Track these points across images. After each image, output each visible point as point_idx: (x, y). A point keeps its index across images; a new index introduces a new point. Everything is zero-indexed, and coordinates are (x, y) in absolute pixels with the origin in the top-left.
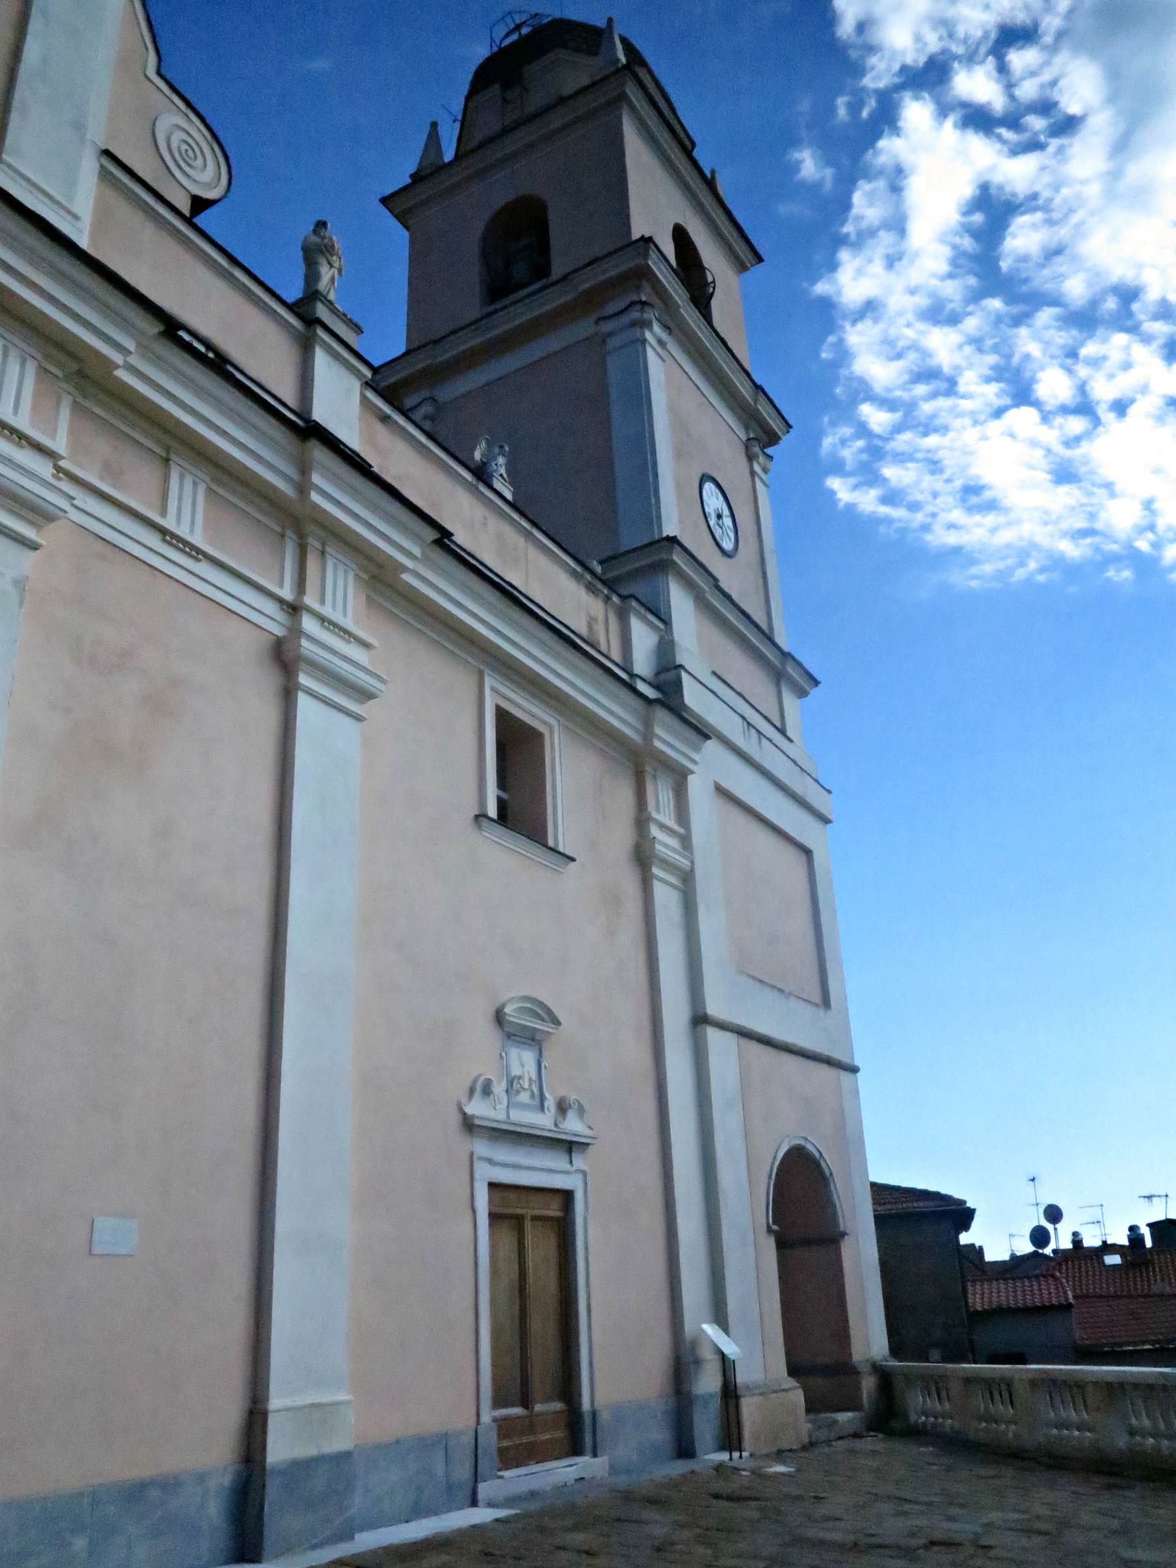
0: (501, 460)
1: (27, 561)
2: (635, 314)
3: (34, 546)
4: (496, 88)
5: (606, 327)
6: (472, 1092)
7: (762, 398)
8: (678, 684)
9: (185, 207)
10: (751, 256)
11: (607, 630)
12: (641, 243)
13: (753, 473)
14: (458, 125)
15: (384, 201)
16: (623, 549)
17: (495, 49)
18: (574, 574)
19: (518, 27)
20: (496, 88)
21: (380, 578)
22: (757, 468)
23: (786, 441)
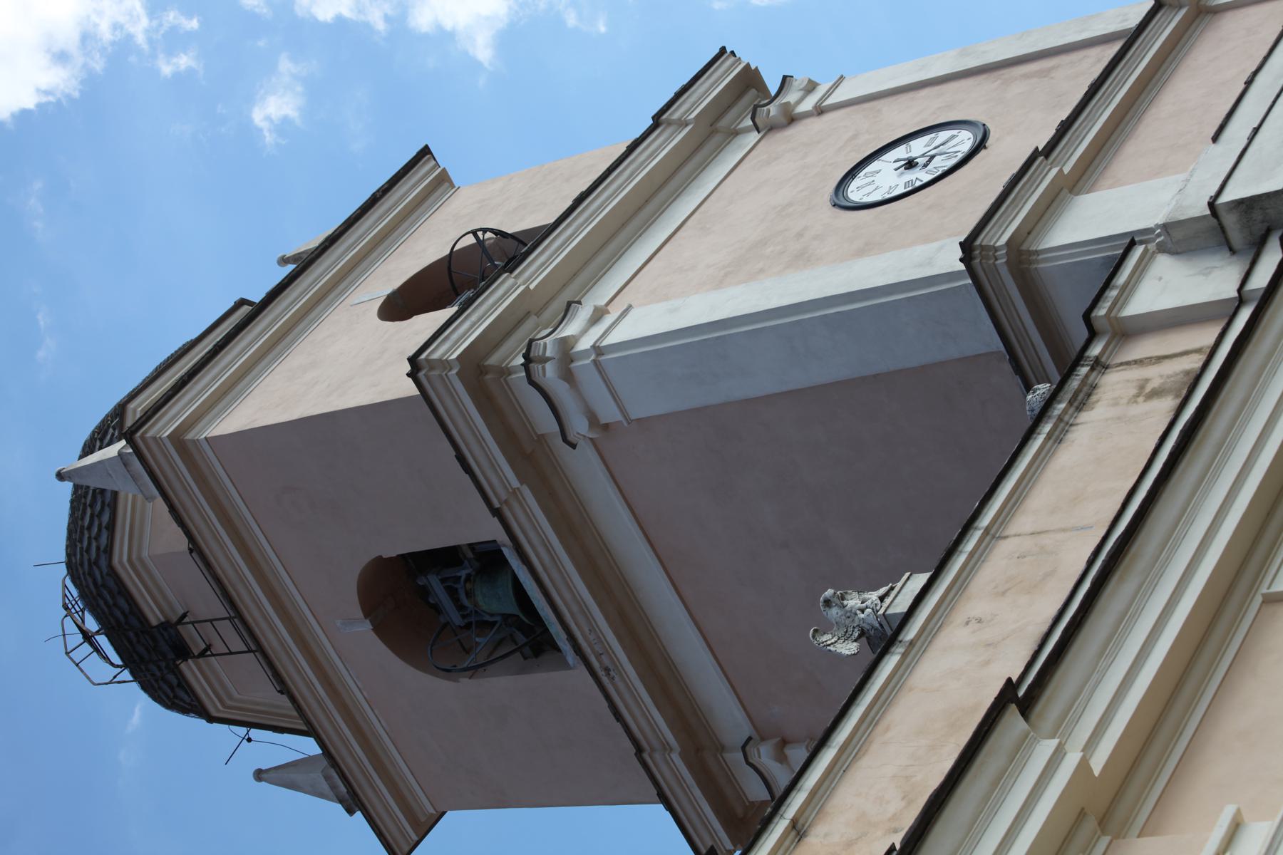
0: (853, 602)
2: (549, 374)
4: (189, 669)
5: (579, 426)
7: (675, 114)
8: (1247, 205)
10: (424, 168)
11: (1160, 359)
12: (421, 375)
13: (820, 111)
14: (254, 733)
16: (998, 344)
17: (126, 675)
18: (1057, 438)
19: (88, 637)
20: (189, 669)
22: (808, 105)
23: (749, 56)
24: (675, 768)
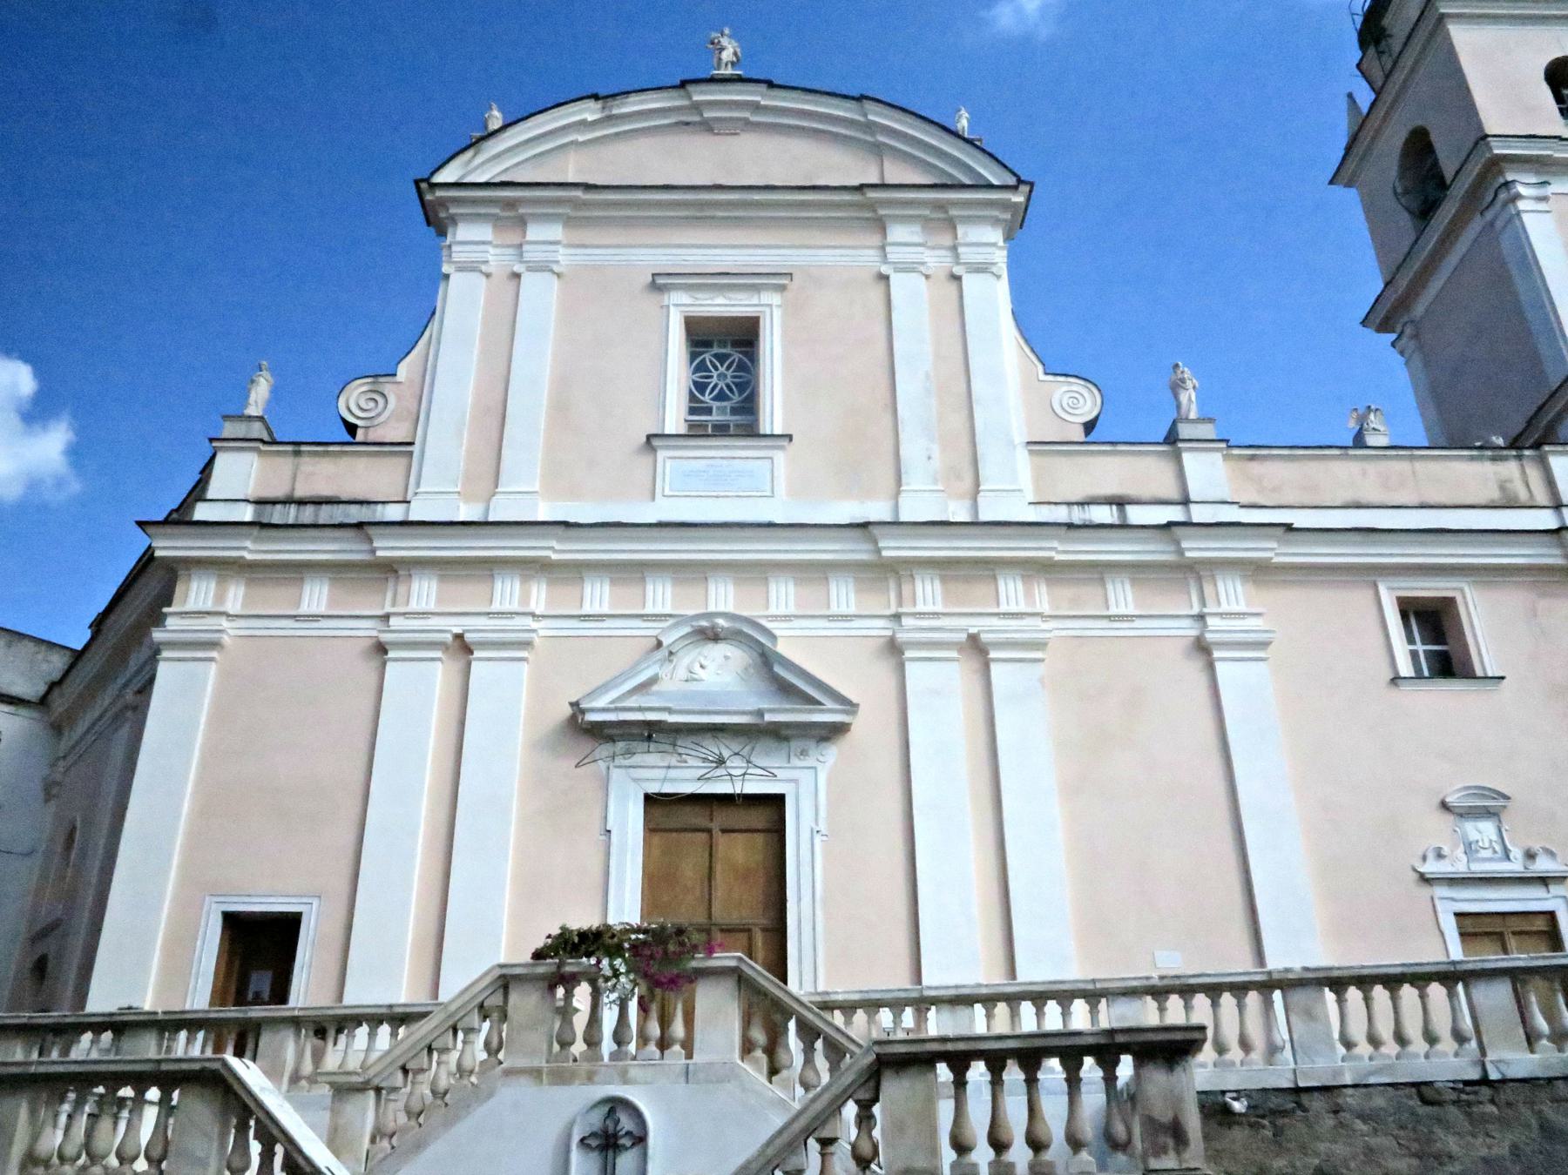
1: (1040, 669)
2: (1503, 196)
3: (1042, 660)
4: (1371, 51)
5: (1489, 215)
6: (1424, 858)
9: (1079, 435)
15: (1331, 182)
17: (1359, 20)
18: (1472, 458)
21: (1258, 572)
24: (1393, 297)
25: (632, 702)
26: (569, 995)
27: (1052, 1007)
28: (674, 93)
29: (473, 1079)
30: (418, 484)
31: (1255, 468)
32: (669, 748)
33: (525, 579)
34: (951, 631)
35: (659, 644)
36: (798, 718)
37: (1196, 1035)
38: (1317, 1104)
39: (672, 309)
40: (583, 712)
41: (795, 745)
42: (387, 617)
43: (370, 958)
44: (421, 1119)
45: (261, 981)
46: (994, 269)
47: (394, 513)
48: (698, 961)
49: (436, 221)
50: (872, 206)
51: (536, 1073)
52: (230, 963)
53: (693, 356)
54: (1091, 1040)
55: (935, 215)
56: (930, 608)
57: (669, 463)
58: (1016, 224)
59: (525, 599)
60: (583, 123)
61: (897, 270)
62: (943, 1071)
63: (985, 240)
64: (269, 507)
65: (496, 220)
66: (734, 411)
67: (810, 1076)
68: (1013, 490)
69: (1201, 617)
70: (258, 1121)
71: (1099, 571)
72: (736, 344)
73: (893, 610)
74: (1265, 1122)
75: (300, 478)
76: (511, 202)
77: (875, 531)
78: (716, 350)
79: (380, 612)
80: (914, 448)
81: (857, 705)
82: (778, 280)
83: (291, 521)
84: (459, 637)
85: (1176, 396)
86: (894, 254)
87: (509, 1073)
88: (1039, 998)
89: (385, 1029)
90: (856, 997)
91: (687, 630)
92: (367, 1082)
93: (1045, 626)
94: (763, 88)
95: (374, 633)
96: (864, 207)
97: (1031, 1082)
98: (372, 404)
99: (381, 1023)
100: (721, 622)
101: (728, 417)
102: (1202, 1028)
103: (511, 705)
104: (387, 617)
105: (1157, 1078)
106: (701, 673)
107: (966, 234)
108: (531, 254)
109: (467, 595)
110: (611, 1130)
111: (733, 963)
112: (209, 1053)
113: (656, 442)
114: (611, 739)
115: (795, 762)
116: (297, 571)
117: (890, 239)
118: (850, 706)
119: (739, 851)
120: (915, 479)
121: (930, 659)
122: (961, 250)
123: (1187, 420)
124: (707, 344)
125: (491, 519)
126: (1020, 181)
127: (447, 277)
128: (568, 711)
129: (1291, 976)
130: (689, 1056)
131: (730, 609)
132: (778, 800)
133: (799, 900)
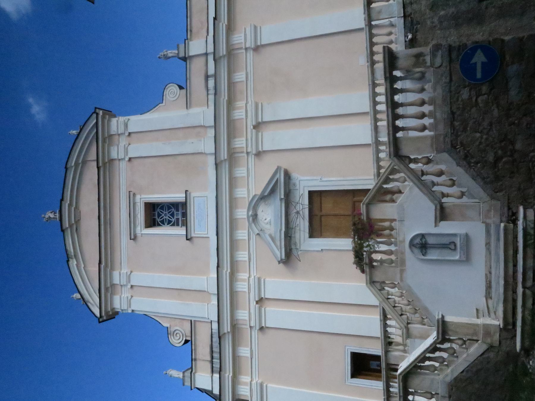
9: (184, 91)
21: (230, 29)
25: (278, 243)
26: (376, 261)
27: (378, 99)
28: (66, 233)
29: (404, 292)
30: (205, 318)
31: (194, 30)
32: (293, 230)
33: (237, 280)
34: (252, 134)
35: (258, 234)
36: (282, 187)
37: (386, 49)
38: (409, 10)
39: (143, 232)
40: (282, 259)
41: (292, 188)
42: (251, 327)
43: (365, 329)
44: (417, 309)
45: (373, 365)
46: (126, 121)
47: (215, 326)
48: (364, 217)
49: (113, 315)
50: (104, 164)
51: (402, 271)
52: (366, 375)
53: (159, 225)
54: (388, 84)
55: (107, 141)
56: (244, 142)
57: (196, 233)
58: (110, 114)
59: (244, 280)
60: (77, 265)
61: (127, 154)
62: (400, 134)
63: (116, 124)
64: (214, 369)
65: (112, 294)
66: (178, 210)
67: (402, 179)
68: (202, 114)
69: (246, 49)
70: (419, 362)
71: (231, 85)
72: (154, 210)
73: (246, 155)
74: (415, 27)
75: (204, 358)
76: (106, 289)
77: (218, 161)
78: (156, 217)
79: (249, 329)
80: (188, 148)
81: (278, 167)
82: (132, 196)
83: (219, 361)
84: (257, 302)
85: (169, 58)
86: (121, 156)
87: (402, 280)
88: (375, 103)
89: (388, 322)
90: (375, 165)
91: (253, 225)
92: (406, 327)
93: (250, 103)
94: (63, 202)
95: (256, 331)
96: (105, 166)
97: (402, 105)
98: (178, 335)
99: (386, 324)
100: (250, 213)
101: (180, 212)
102: (384, 47)
103: (280, 284)
104: (251, 327)
105: (401, 63)
106: (268, 219)
107: (114, 131)
108: (123, 282)
109: (242, 300)
110: (420, 246)
111: (365, 206)
112: (397, 380)
113: (189, 237)
114: (291, 250)
115: (298, 187)
116: (236, 358)
117: (116, 157)
118: (278, 169)
119: (328, 206)
120: (201, 149)
121: (262, 142)
122: (119, 133)
123: (178, 54)
124: (154, 219)
125: (216, 293)
126: (95, 112)
127: (133, 311)
128: (281, 264)
129: (367, 18)
130: (395, 220)
131: (246, 210)
132: (311, 193)
133: (344, 185)
